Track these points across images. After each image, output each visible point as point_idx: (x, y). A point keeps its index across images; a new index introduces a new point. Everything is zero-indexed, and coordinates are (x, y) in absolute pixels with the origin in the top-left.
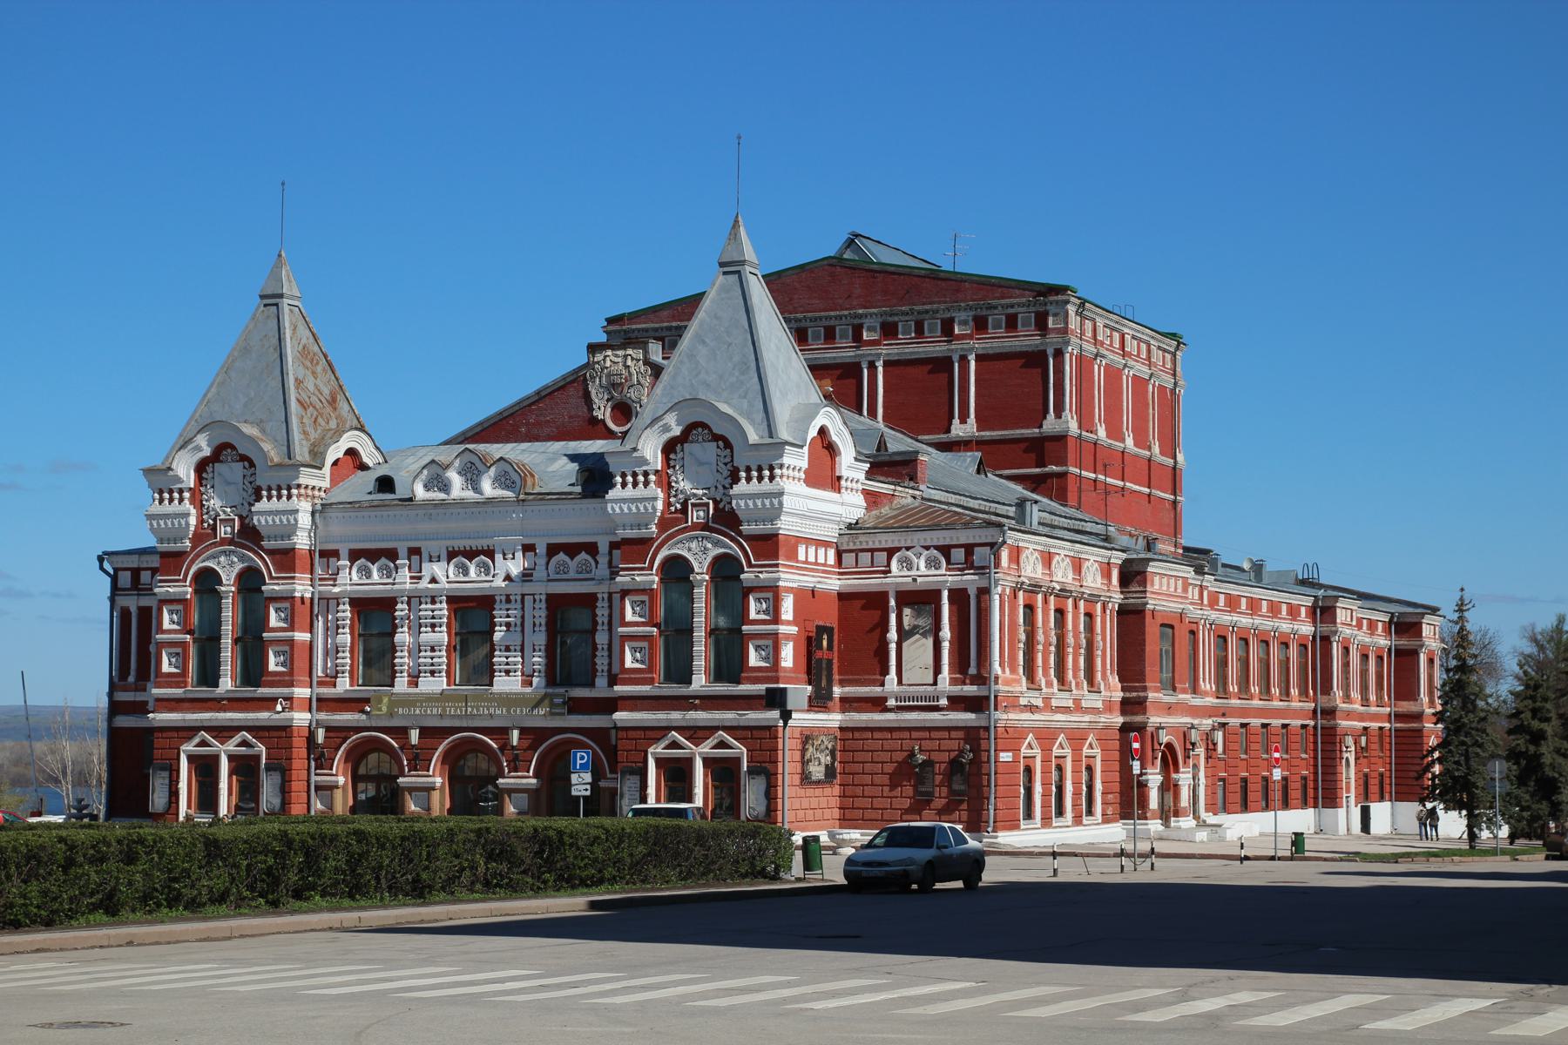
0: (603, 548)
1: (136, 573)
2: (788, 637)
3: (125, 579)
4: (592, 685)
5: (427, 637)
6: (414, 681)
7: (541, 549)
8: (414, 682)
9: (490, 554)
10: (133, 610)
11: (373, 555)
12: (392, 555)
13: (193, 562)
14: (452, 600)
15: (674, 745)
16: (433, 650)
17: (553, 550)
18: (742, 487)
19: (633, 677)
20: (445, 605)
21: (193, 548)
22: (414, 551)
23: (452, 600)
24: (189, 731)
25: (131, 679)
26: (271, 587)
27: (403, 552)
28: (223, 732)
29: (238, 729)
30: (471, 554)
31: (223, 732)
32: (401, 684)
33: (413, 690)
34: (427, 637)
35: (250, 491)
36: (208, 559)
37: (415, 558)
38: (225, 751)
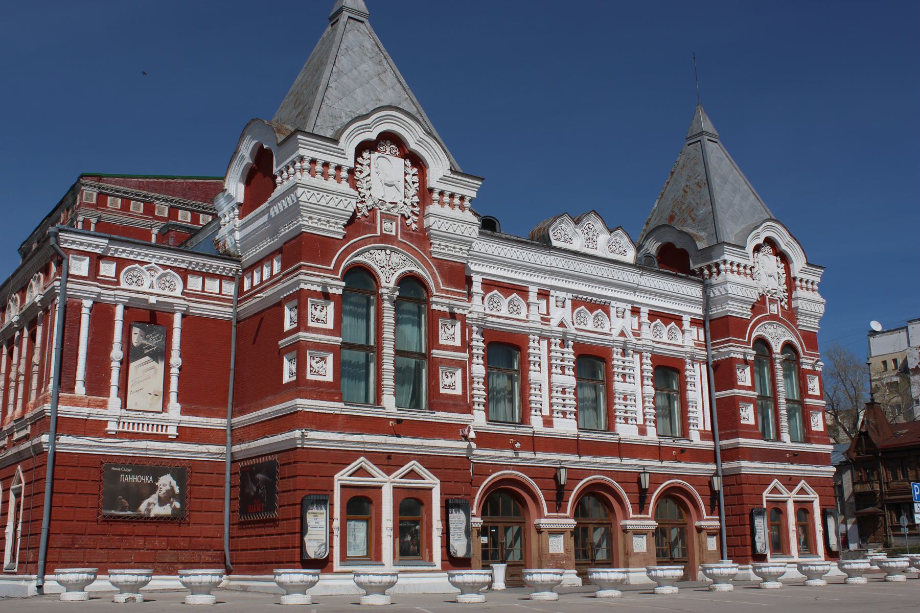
0: (686, 325)
1: (96, 260)
2: (817, 409)
3: (80, 267)
4: (685, 435)
5: (558, 379)
6: (548, 422)
7: (645, 311)
8: (548, 422)
9: (606, 308)
10: (87, 304)
11: (507, 289)
12: (523, 292)
13: (346, 252)
14: (577, 346)
15: (775, 490)
16: (563, 392)
17: (653, 315)
18: (799, 293)
19: (749, 432)
20: (571, 350)
21: (346, 238)
22: (544, 294)
23: (577, 346)
24: (343, 458)
25: (80, 389)
26: (440, 303)
27: (533, 291)
28: (389, 462)
29: (407, 458)
30: (592, 307)
31: (389, 462)
32: (536, 424)
33: (548, 430)
34: (558, 379)
35: (412, 191)
36: (357, 255)
37: (543, 303)
38: (387, 484)
